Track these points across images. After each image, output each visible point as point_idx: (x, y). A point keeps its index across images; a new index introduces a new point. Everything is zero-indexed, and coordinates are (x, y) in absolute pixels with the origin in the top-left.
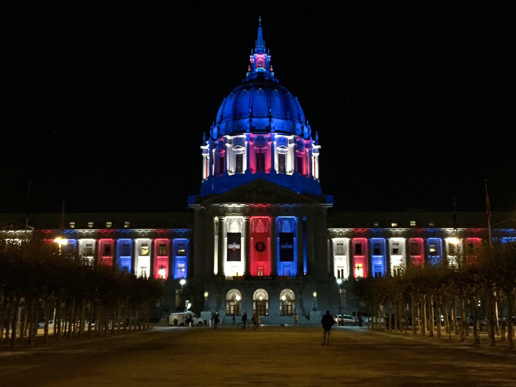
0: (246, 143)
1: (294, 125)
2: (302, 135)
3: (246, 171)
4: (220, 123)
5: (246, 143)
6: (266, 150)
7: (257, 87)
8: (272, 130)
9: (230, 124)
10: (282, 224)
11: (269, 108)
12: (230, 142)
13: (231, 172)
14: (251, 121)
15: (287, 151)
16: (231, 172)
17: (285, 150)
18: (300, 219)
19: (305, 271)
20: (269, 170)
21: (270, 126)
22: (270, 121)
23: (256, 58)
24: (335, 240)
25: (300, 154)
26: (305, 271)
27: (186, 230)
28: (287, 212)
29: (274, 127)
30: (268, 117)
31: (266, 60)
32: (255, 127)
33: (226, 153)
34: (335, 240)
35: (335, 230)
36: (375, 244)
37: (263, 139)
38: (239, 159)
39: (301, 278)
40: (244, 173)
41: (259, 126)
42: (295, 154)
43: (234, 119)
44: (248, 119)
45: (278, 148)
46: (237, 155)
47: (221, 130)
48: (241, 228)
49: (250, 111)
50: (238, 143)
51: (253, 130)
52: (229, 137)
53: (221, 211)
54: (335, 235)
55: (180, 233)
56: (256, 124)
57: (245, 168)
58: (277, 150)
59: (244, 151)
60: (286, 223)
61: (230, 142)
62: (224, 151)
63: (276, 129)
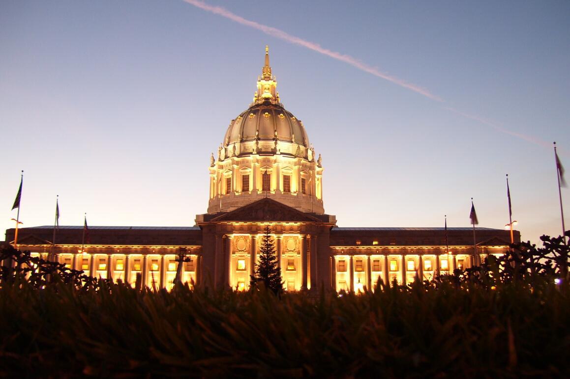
1: (299, 147)
2: (306, 158)
3: (252, 191)
4: (228, 145)
5: (252, 165)
6: (271, 171)
7: (264, 111)
8: (278, 152)
9: (238, 145)
10: (287, 241)
11: (275, 131)
12: (237, 163)
13: (237, 192)
14: (257, 143)
16: (237, 192)
17: (290, 172)
18: (305, 238)
19: (309, 287)
20: (274, 190)
21: (275, 148)
22: (276, 143)
23: (263, 84)
24: (338, 258)
26: (309, 287)
27: (195, 247)
28: (291, 230)
29: (279, 151)
30: (274, 139)
31: (272, 85)
32: (261, 149)
34: (338, 258)
35: (337, 248)
36: (374, 261)
37: (269, 161)
38: (245, 180)
39: (305, 293)
41: (265, 148)
42: (299, 175)
43: (242, 141)
44: (255, 142)
45: (283, 170)
46: (243, 176)
47: (228, 152)
48: (248, 245)
49: (257, 134)
51: (259, 152)
52: (236, 159)
53: (229, 228)
54: (337, 253)
55: (189, 250)
56: (263, 146)
57: (251, 188)
59: (250, 172)
60: (291, 241)
61: (237, 163)
62: (231, 172)
63: (281, 151)
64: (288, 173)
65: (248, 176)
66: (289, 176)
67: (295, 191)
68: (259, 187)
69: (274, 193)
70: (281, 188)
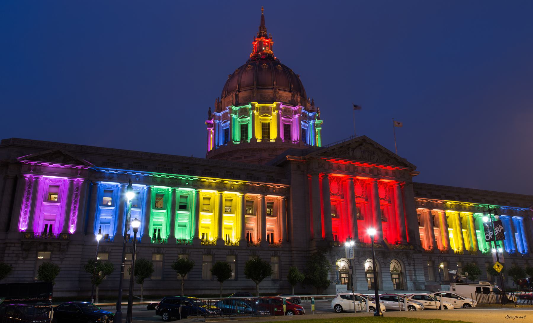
0: (251, 113)
5: (251, 113)
6: (271, 120)
15: (292, 122)
16: (236, 141)
22: (275, 92)
25: (304, 126)
30: (272, 89)
33: (231, 124)
40: (249, 141)
45: (282, 118)
46: (242, 125)
50: (244, 113)
57: (250, 136)
58: (283, 120)
59: (249, 120)
62: (229, 122)
64: (289, 122)
65: (246, 126)
66: (290, 125)
67: (296, 140)
68: (259, 136)
69: (274, 141)
70: (282, 137)
